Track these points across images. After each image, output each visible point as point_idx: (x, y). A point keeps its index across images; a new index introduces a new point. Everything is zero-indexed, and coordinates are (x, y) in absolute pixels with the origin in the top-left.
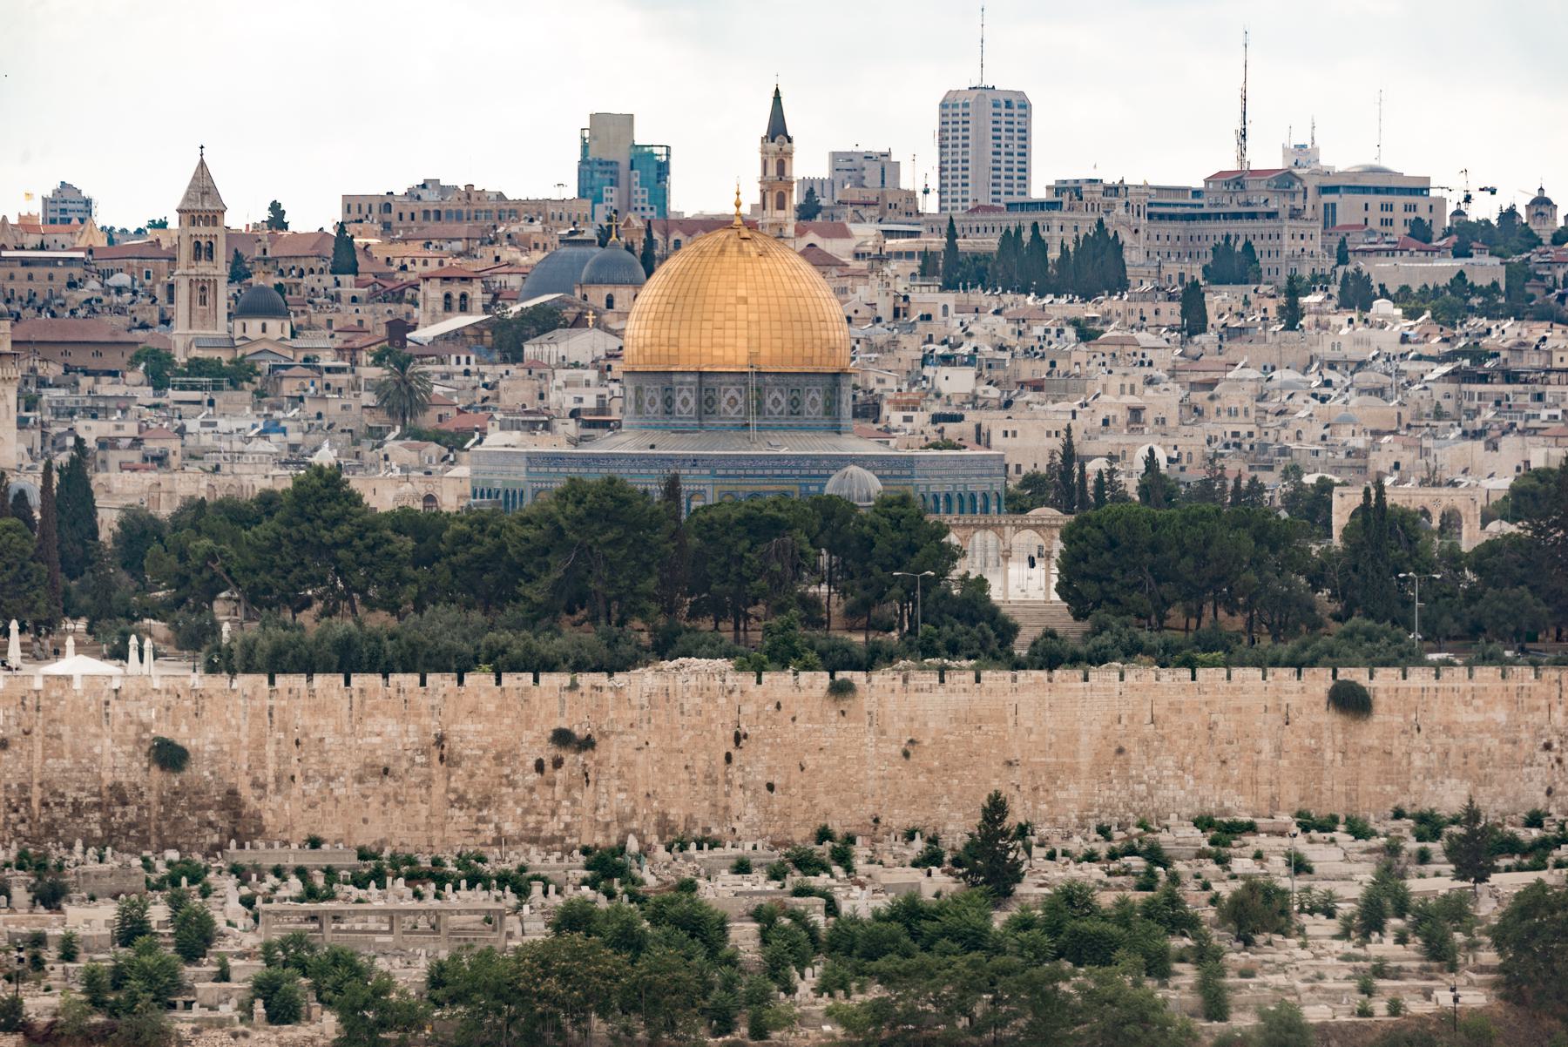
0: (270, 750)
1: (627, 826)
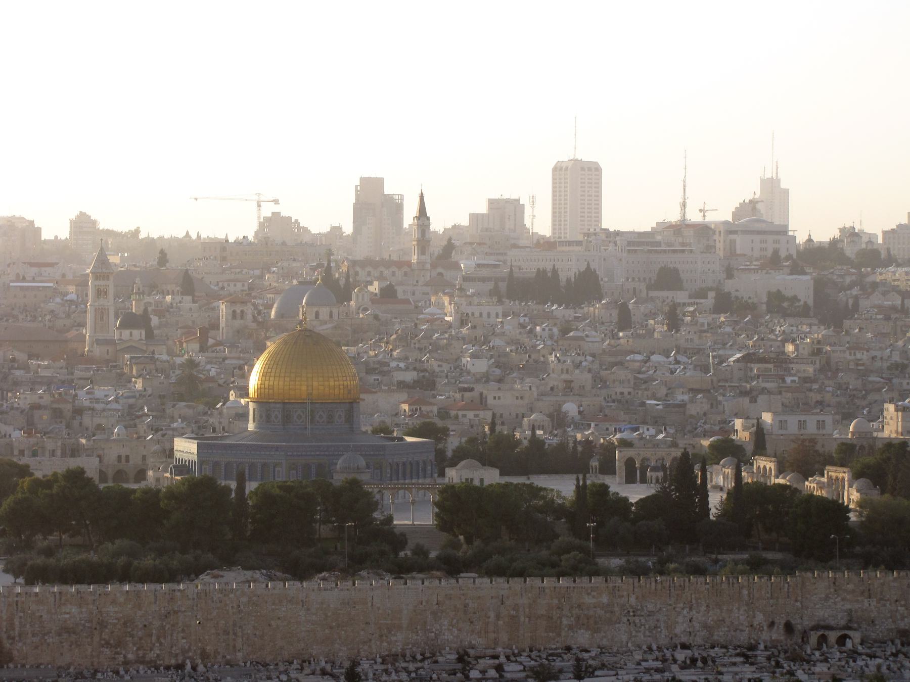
0: (17, 622)
1: (186, 655)
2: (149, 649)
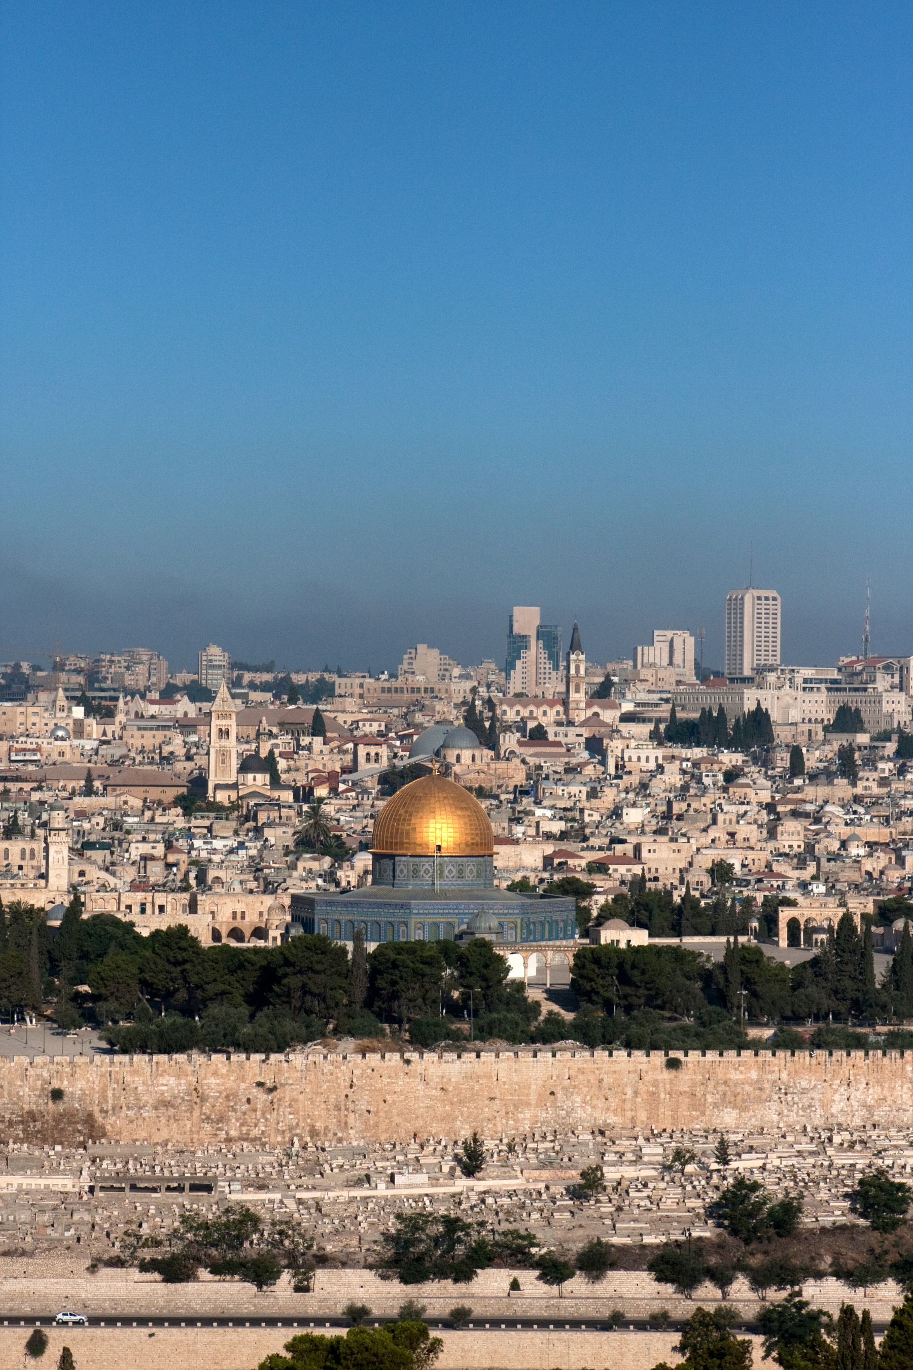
0: (110, 1094)
1: (294, 1132)
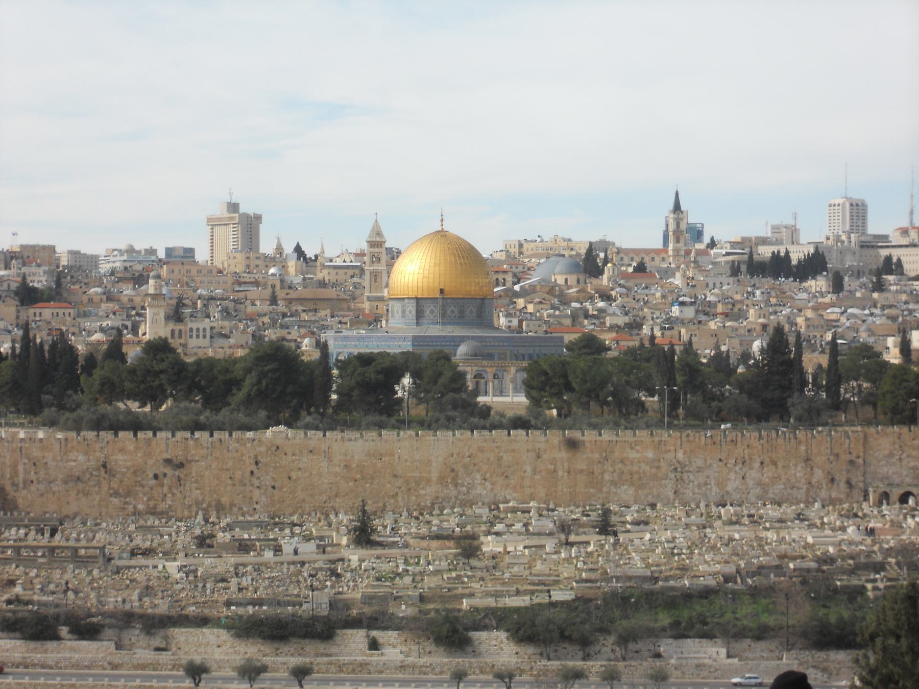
0: (21, 468)
2: (160, 499)
